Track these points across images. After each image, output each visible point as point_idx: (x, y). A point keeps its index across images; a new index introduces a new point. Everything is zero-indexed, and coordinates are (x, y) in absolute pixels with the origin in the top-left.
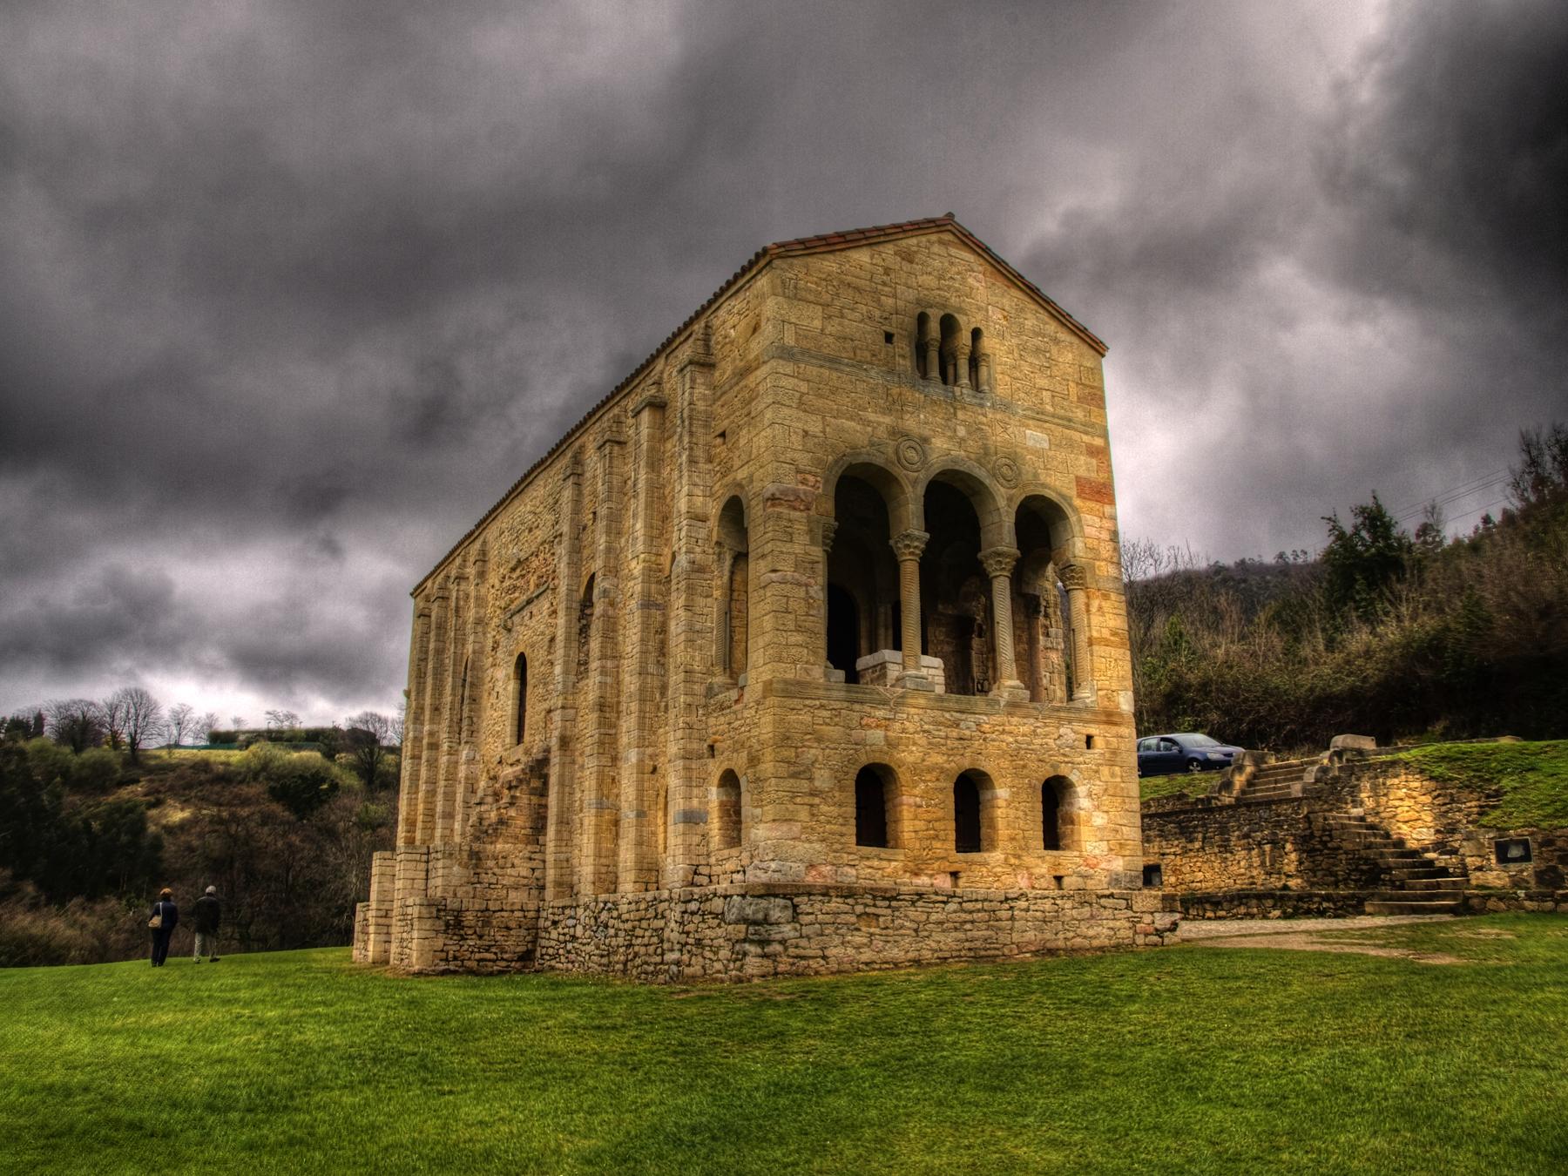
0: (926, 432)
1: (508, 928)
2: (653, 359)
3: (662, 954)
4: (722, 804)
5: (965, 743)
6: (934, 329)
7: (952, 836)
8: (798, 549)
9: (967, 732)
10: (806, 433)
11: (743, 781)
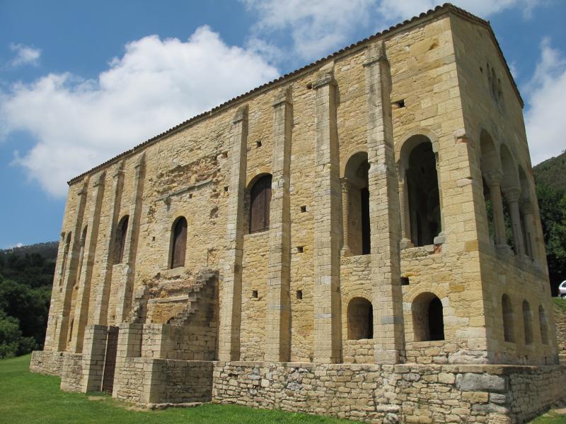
1: (198, 378)
2: (323, 61)
3: (376, 404)
4: (414, 313)
11: (445, 302)
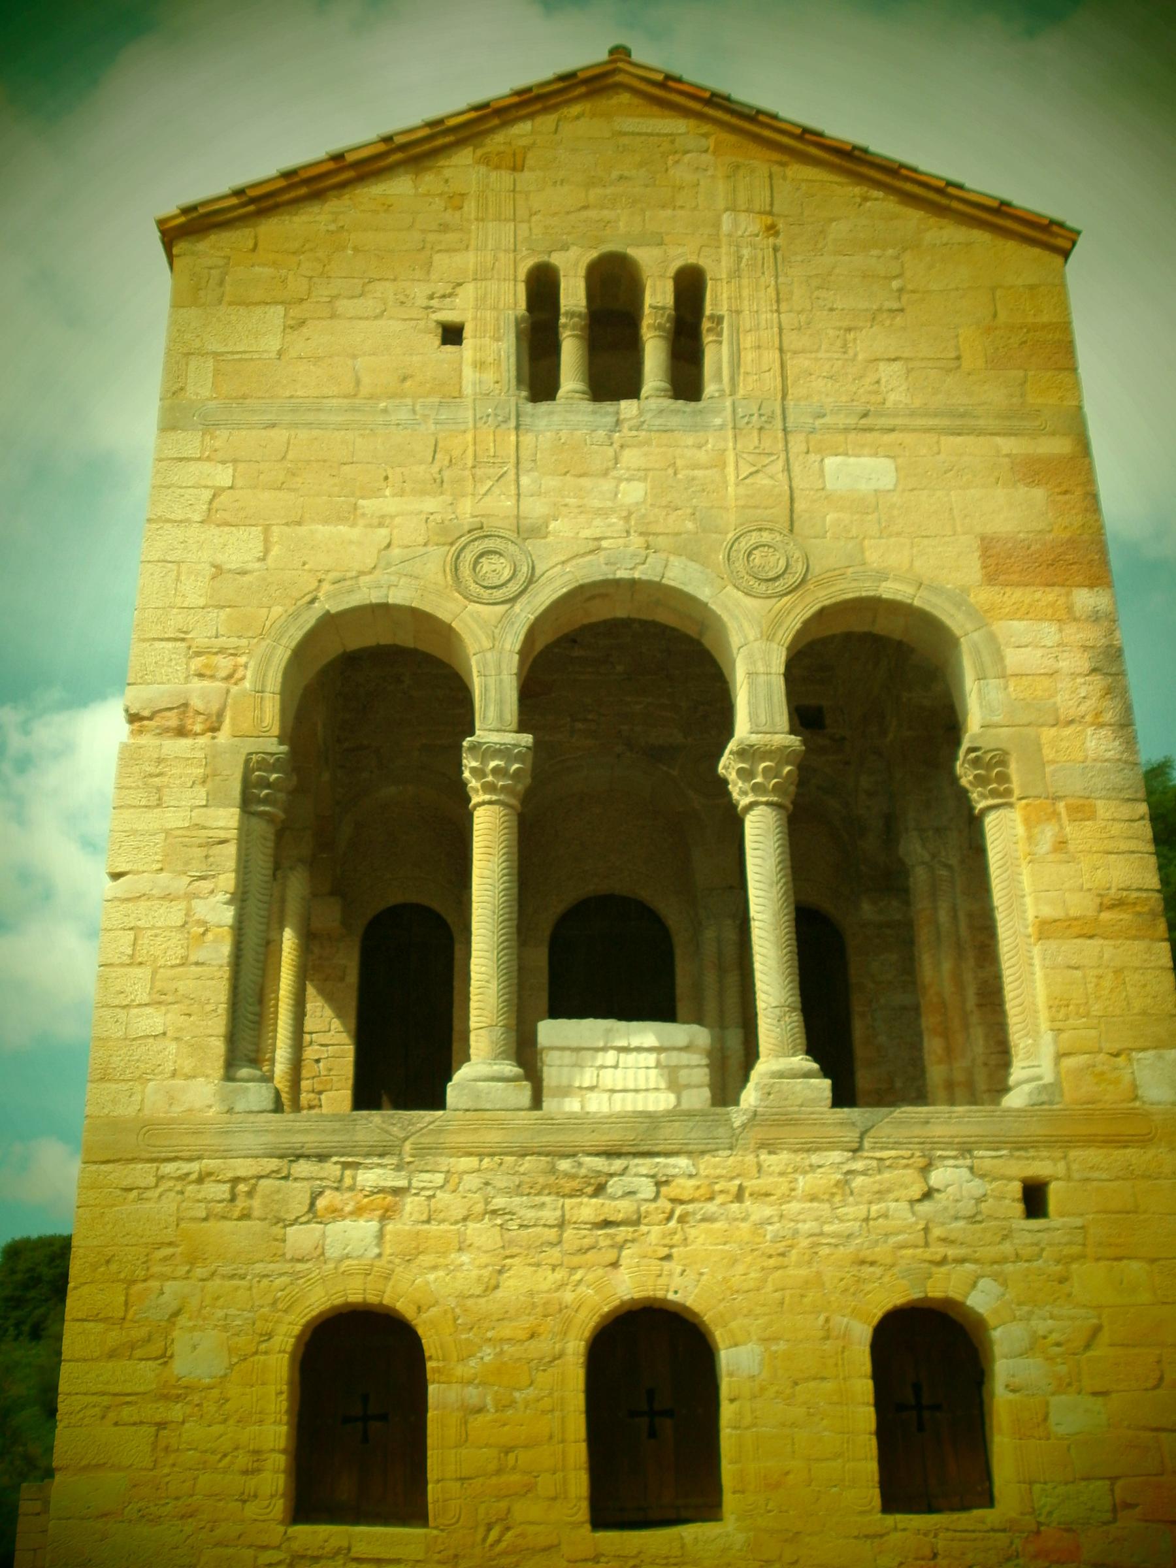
0: (535, 509)
5: (623, 1232)
6: (573, 296)
7: (579, 1483)
8: (174, 819)
9: (623, 1208)
10: (219, 570)
